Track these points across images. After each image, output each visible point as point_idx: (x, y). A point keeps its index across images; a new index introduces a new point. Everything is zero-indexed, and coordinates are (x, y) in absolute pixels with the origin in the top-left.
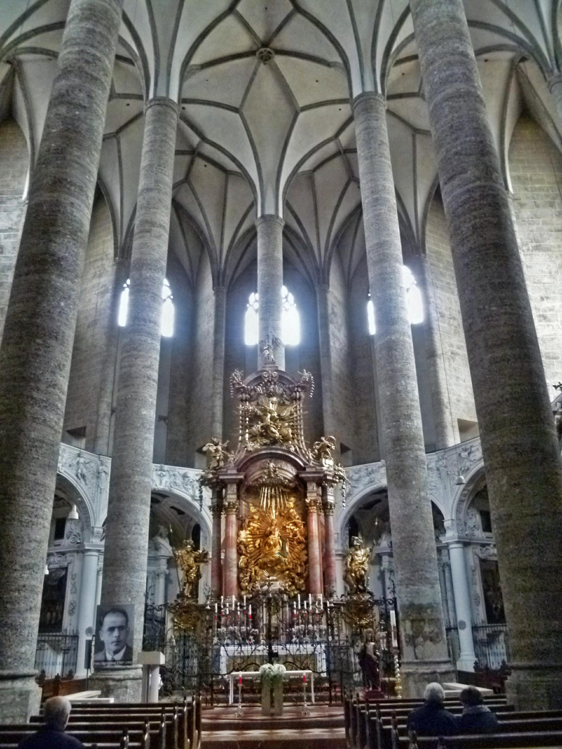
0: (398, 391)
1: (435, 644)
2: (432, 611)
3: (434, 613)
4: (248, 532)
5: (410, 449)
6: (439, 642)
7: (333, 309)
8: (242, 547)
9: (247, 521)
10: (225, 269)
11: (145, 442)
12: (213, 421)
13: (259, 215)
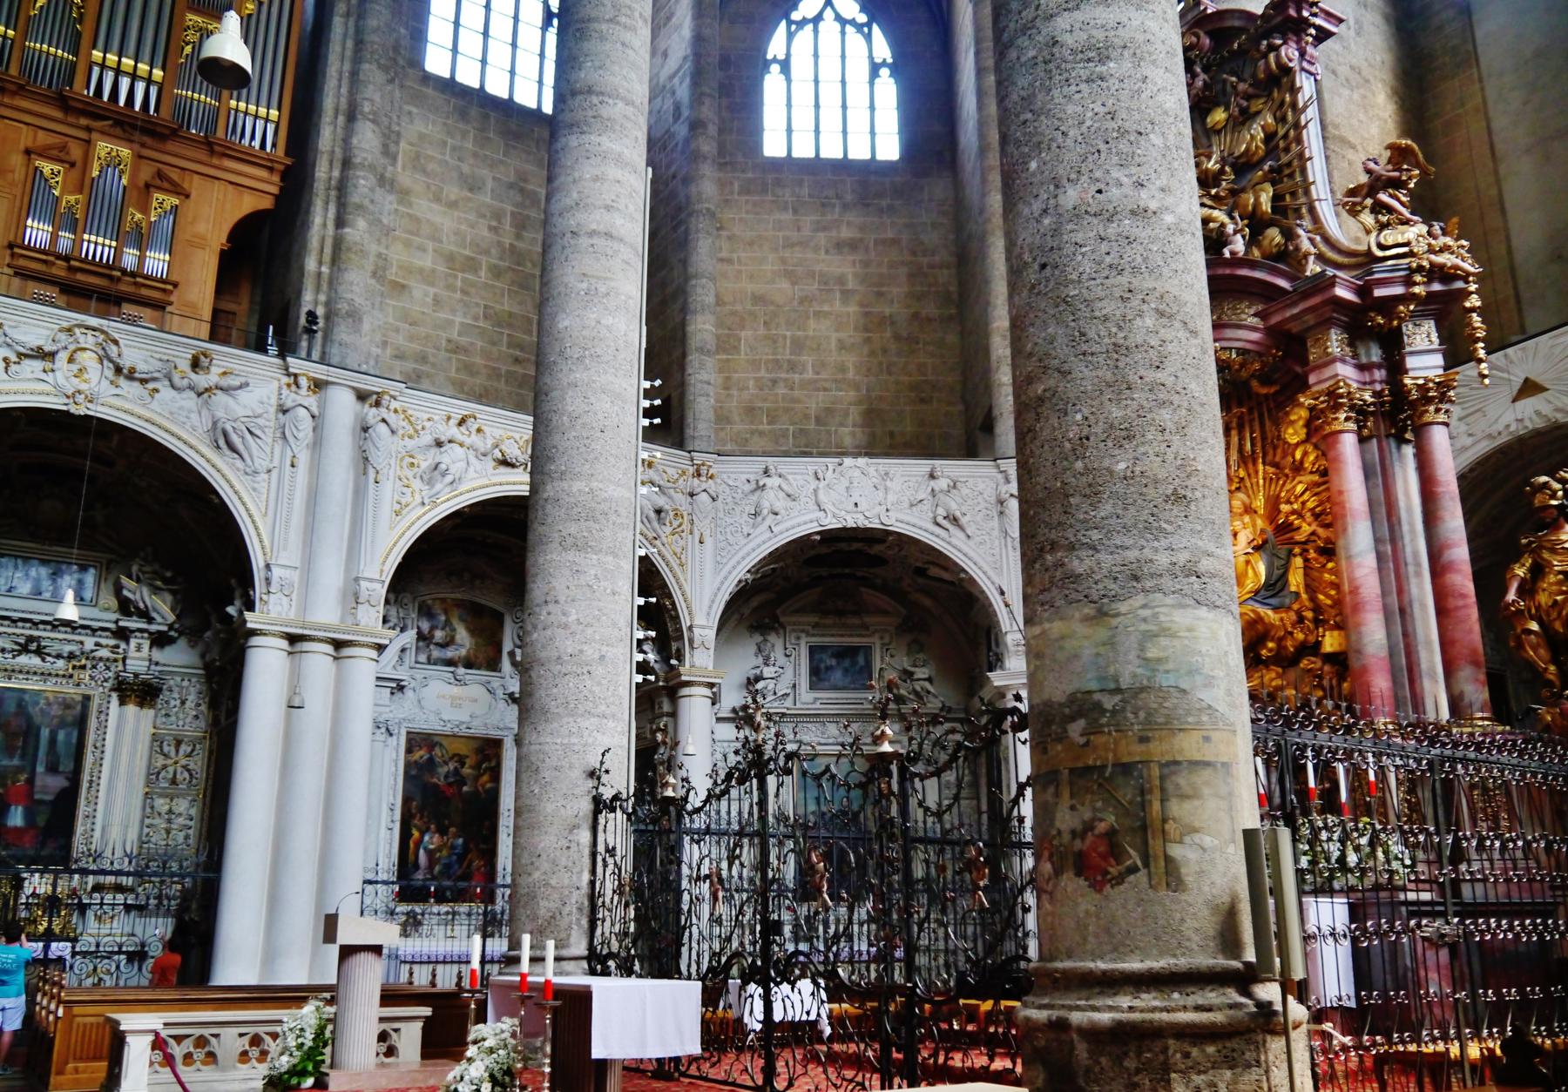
1: (1097, 886)
2: (1093, 730)
3: (1098, 740)
6: (1119, 880)
11: (570, 393)
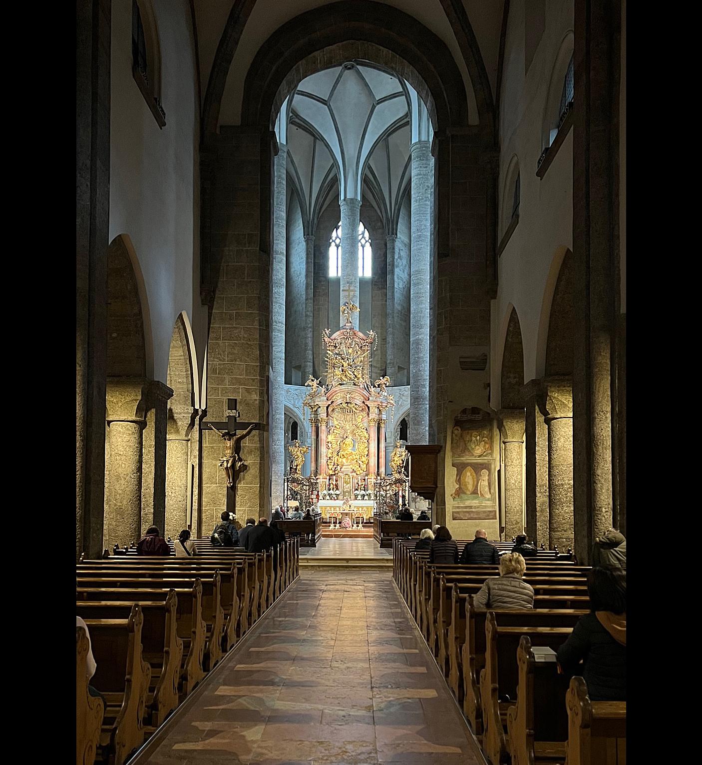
0: (420, 371)
4: (333, 436)
5: (423, 404)
7: (399, 253)
8: (330, 445)
9: (332, 430)
10: (313, 219)
12: (306, 350)
13: (342, 198)
